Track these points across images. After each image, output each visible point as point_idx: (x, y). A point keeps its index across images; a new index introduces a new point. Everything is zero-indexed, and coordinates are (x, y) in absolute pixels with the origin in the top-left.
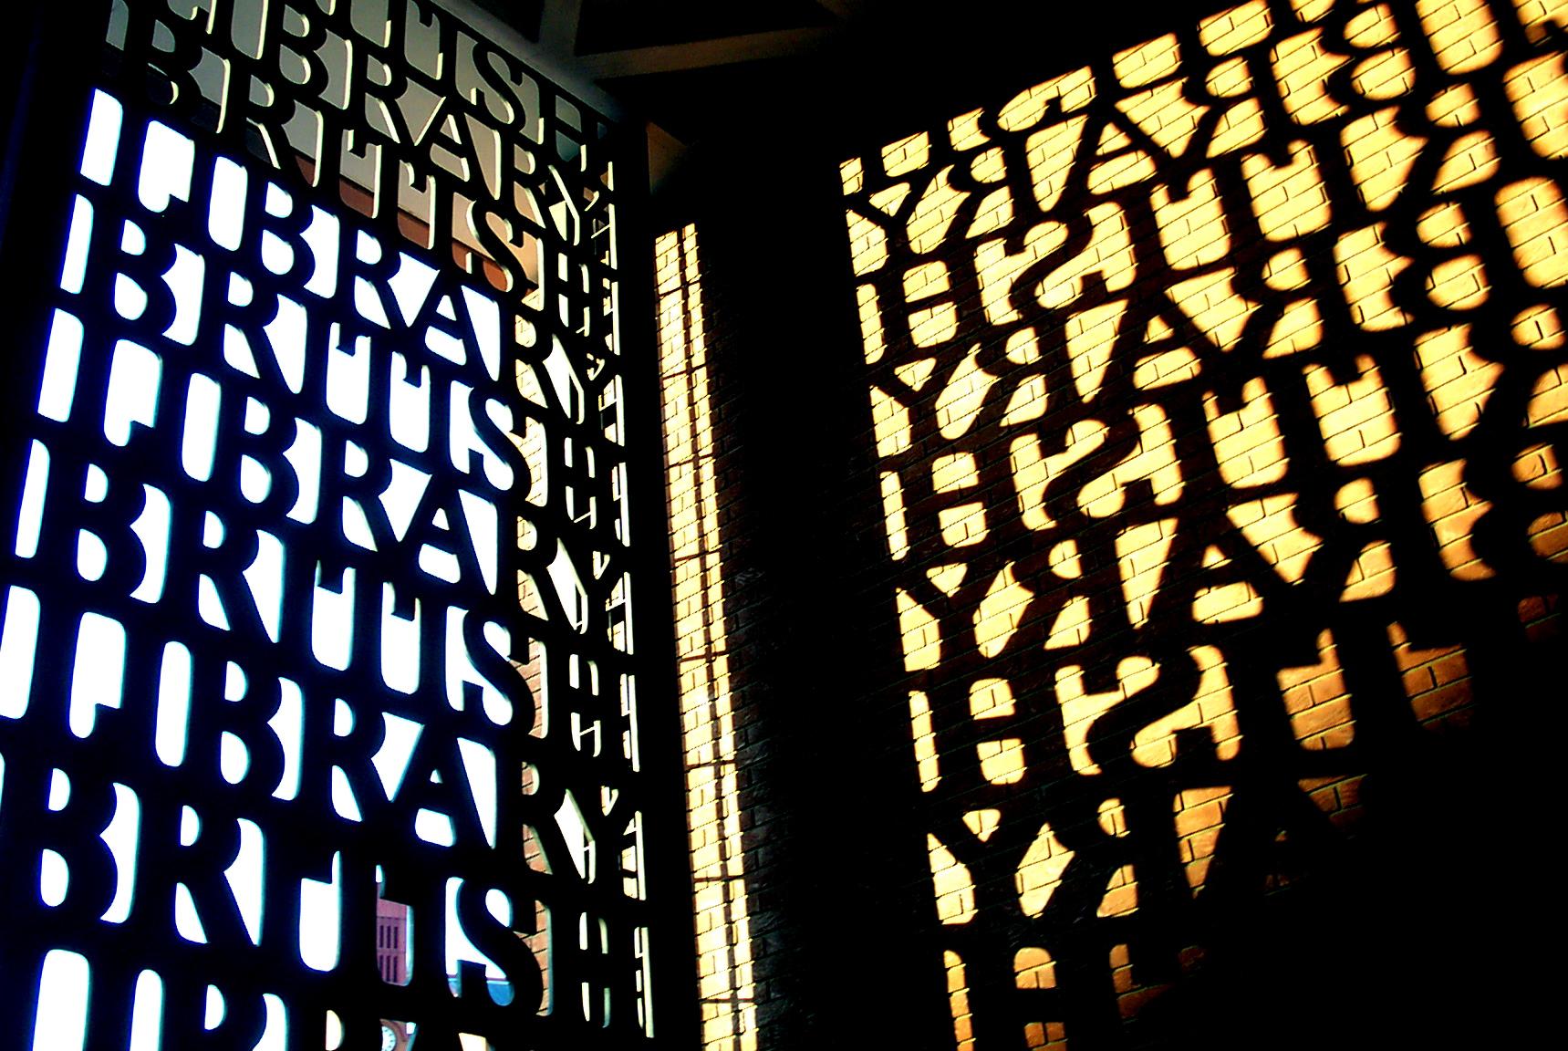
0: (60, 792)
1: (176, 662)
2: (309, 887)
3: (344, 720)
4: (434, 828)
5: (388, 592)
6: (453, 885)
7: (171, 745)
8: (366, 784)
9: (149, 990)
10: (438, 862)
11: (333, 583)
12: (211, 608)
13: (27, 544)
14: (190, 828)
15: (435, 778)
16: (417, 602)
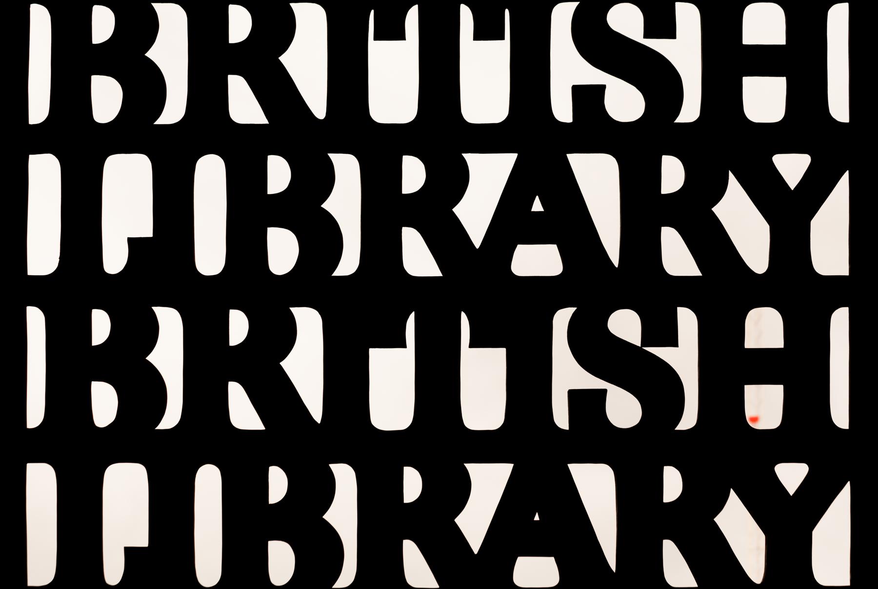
0: (101, 326)
1: (210, 176)
2: (378, 357)
3: (413, 174)
4: (538, 260)
5: (466, 15)
6: (562, 318)
7: (210, 255)
8: (445, 237)
9: (208, 482)
10: (544, 293)
11: (392, 31)
12: (244, 105)
13: (39, 109)
14: (238, 326)
15: (537, 206)
16: (507, 12)
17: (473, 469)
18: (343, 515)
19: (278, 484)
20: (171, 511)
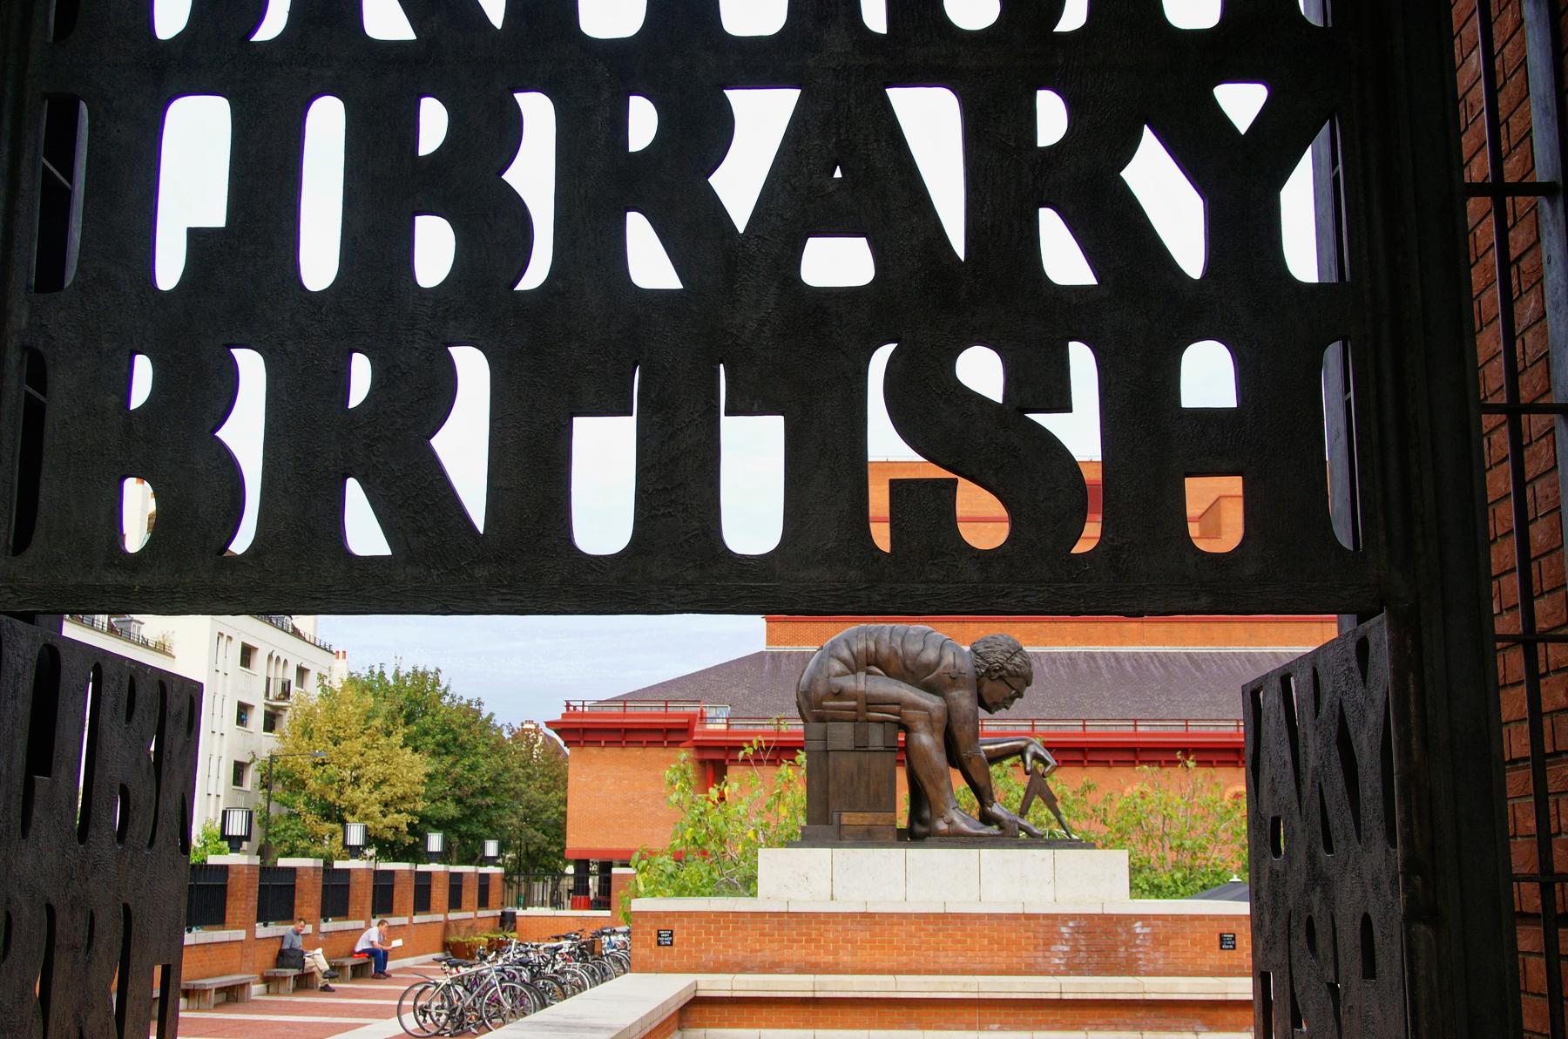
9: (326, 123)
17: (737, 98)
18: (533, 174)
19: (433, 124)
20: (264, 173)
